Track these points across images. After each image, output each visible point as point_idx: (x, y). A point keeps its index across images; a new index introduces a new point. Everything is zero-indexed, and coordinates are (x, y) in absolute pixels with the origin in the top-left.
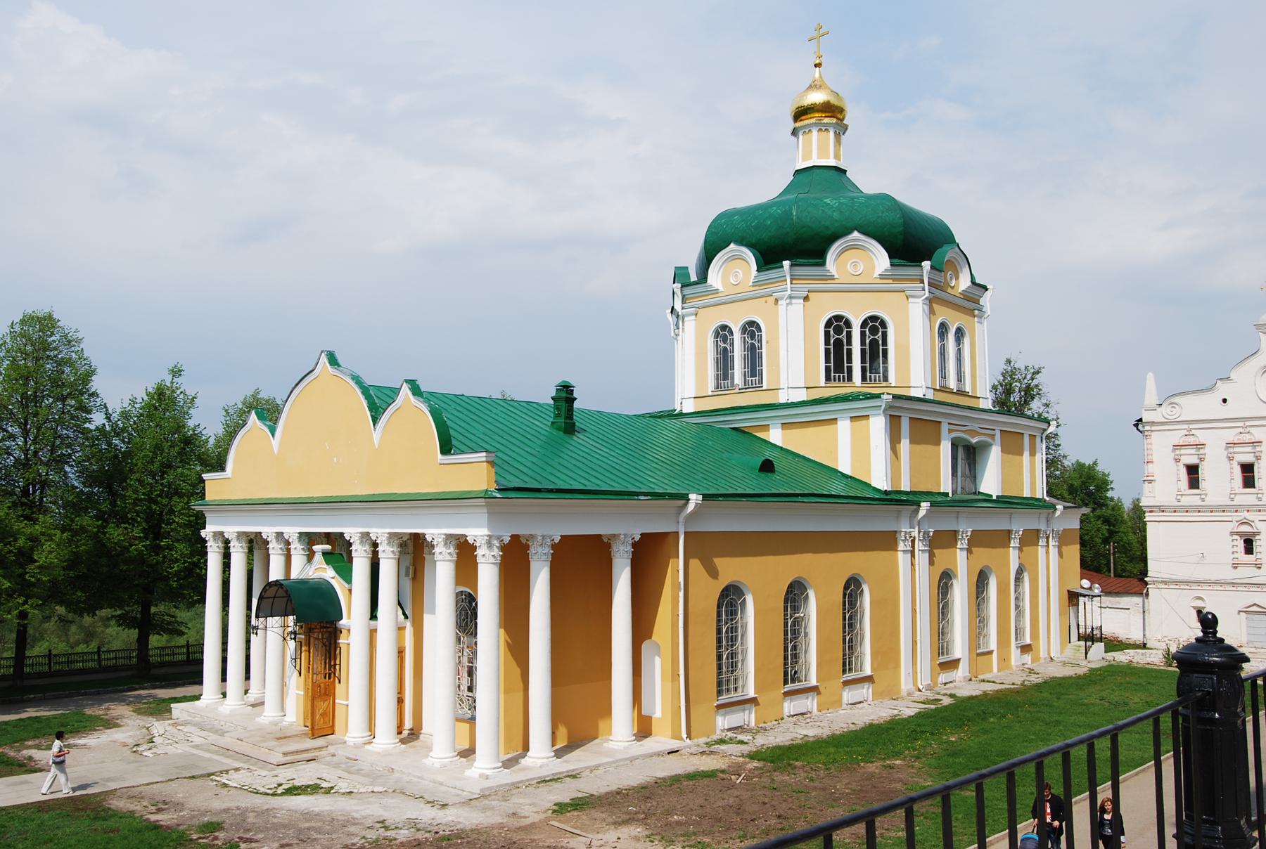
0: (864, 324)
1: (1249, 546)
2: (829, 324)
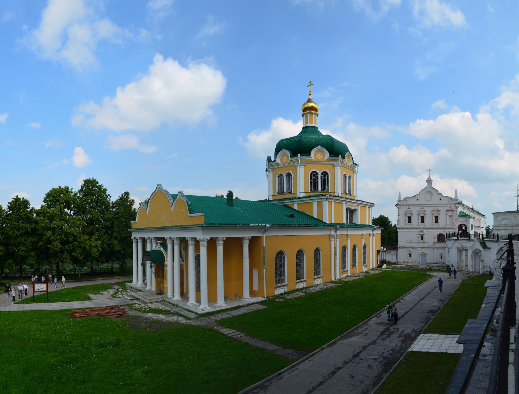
0: (322, 174)
1: (422, 238)
2: (311, 174)
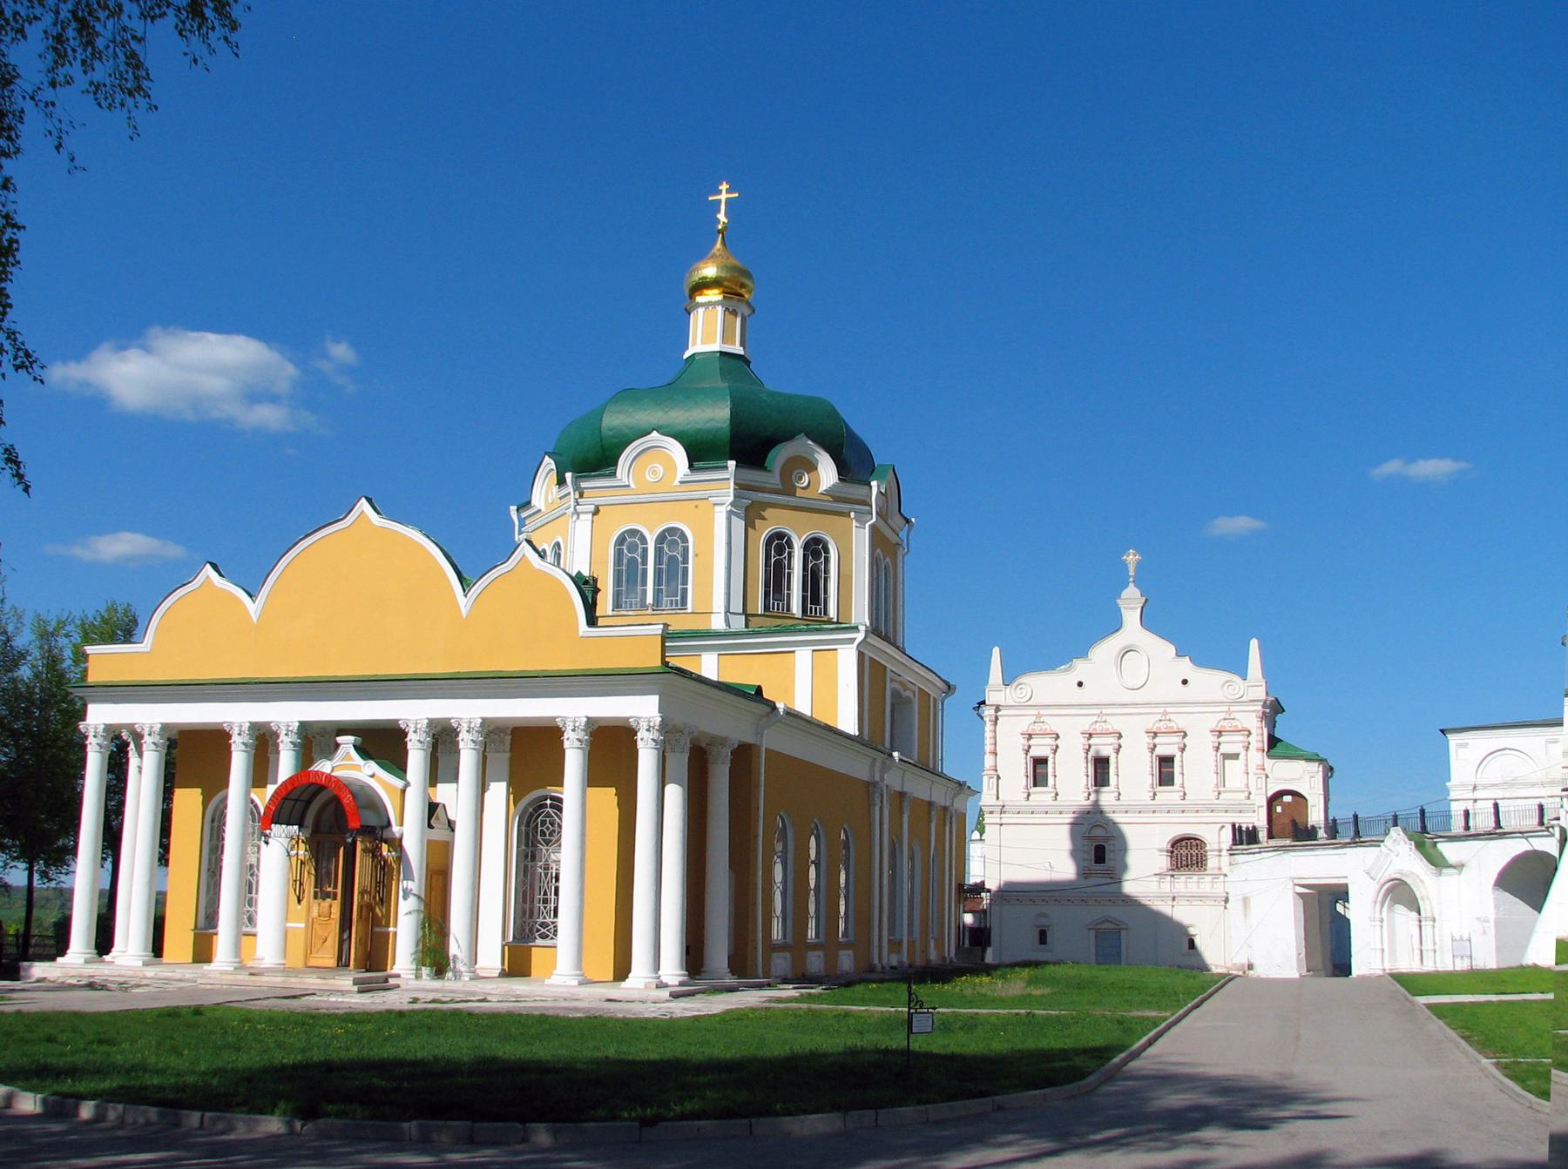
0: (806, 546)
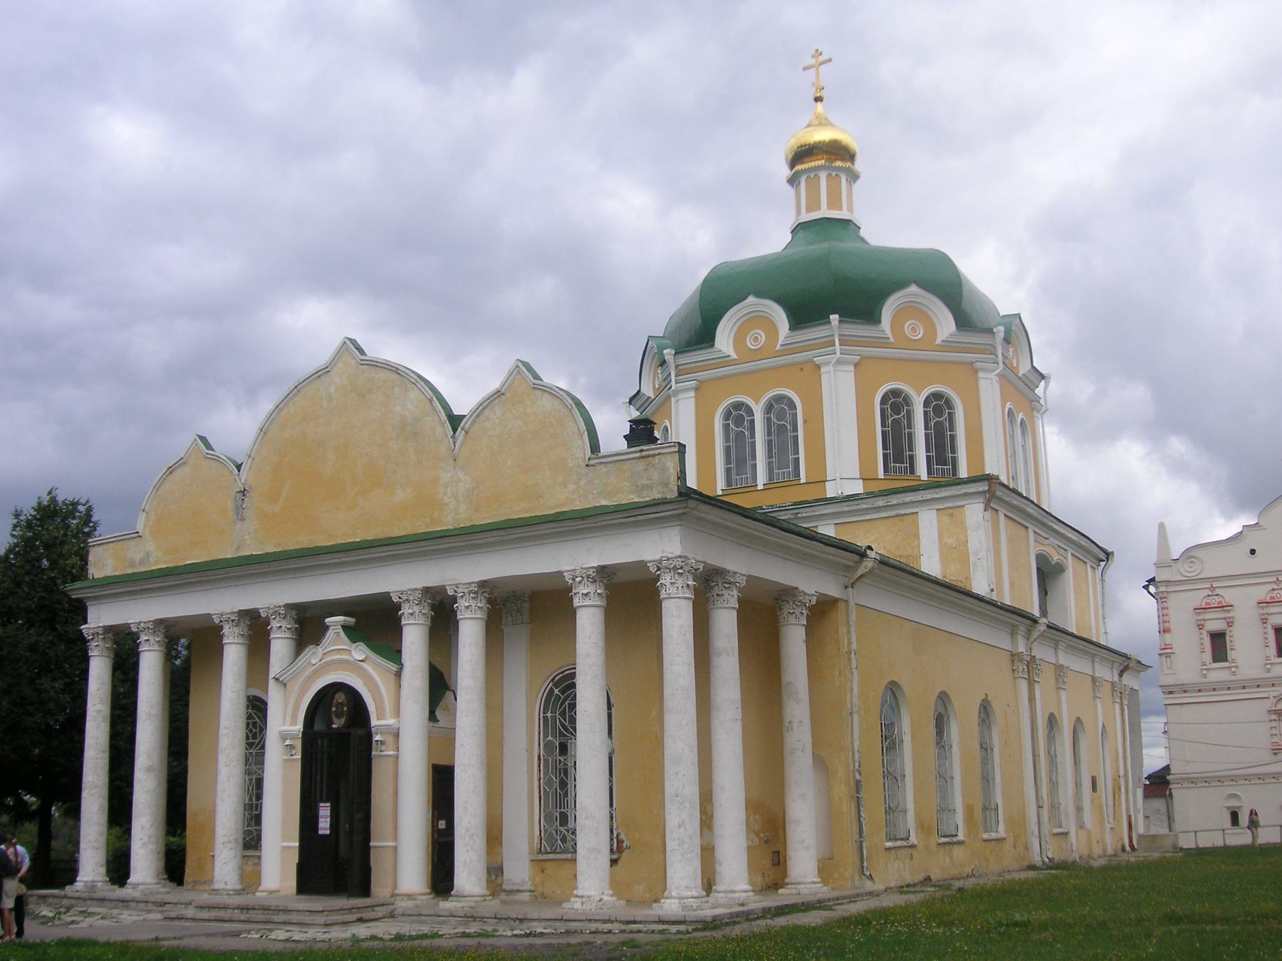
0: (927, 403)
2: (884, 400)
